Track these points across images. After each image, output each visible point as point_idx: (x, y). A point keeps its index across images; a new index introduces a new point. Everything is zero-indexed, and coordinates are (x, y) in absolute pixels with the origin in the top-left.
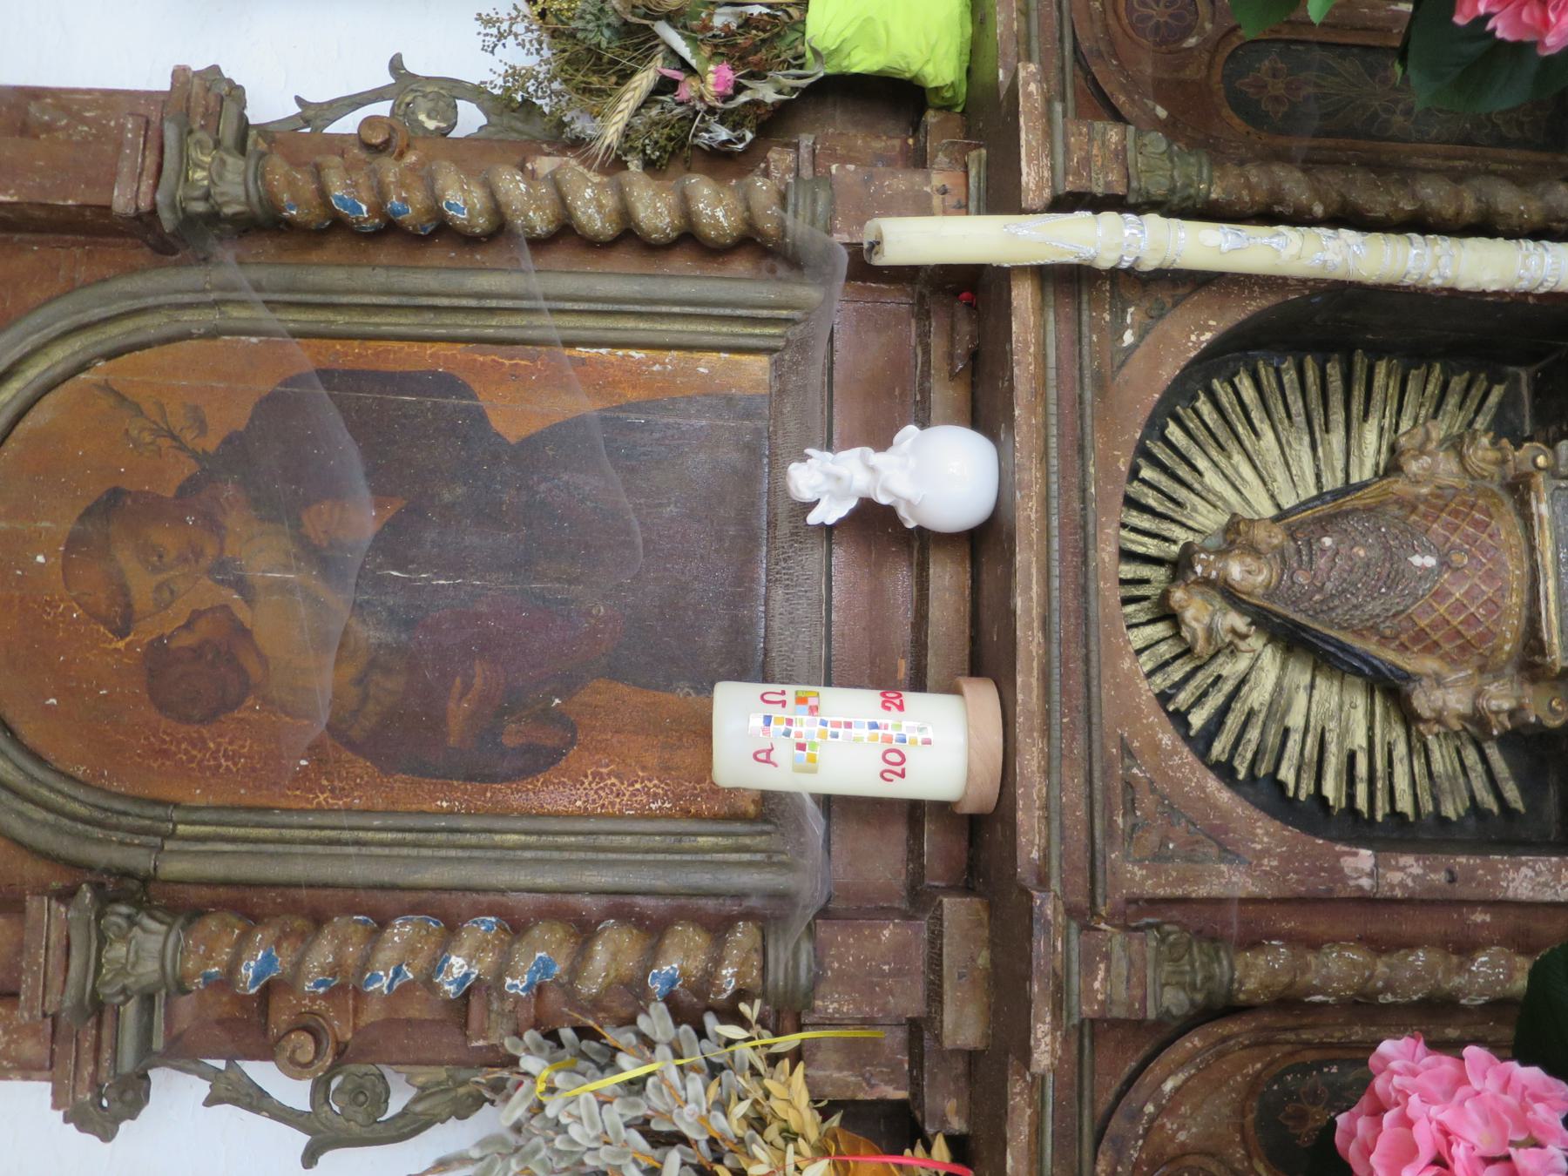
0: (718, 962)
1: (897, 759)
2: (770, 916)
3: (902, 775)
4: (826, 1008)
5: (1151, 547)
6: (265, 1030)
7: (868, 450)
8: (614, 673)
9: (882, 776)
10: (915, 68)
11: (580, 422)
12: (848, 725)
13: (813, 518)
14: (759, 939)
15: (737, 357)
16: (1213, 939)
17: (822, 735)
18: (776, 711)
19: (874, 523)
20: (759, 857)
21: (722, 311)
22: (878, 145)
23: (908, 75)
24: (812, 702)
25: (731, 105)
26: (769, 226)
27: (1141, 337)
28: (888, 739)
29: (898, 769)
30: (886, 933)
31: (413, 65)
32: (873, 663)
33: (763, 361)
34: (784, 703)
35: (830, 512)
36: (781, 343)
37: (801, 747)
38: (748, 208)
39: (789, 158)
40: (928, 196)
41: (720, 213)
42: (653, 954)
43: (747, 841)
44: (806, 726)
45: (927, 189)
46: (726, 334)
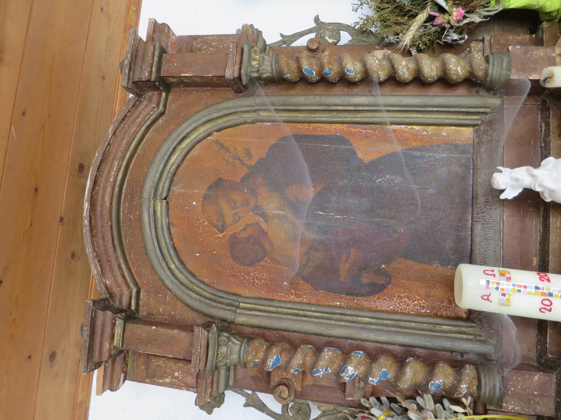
0: (459, 381)
1: (548, 303)
2: (483, 363)
3: (550, 310)
4: (508, 407)
6: (269, 383)
7: (531, 168)
8: (407, 256)
9: (540, 310)
10: (541, 4)
11: (394, 155)
12: (525, 287)
13: (502, 197)
14: (476, 373)
15: (459, 128)
17: (513, 290)
18: (491, 279)
19: (530, 199)
20: (470, 337)
21: (454, 109)
22: (519, 38)
23: (537, 7)
24: (507, 275)
25: (461, 24)
26: (480, 74)
28: (543, 294)
29: (548, 308)
30: (536, 377)
31: (322, 19)
32: (521, 258)
33: (470, 129)
34: (494, 275)
35: (510, 194)
36: (480, 122)
37: (504, 295)
38: (471, 66)
39: (480, 45)
40: (554, 58)
41: (459, 69)
42: (431, 374)
43: (464, 329)
44: (505, 285)
45: (554, 55)
46: (455, 119)
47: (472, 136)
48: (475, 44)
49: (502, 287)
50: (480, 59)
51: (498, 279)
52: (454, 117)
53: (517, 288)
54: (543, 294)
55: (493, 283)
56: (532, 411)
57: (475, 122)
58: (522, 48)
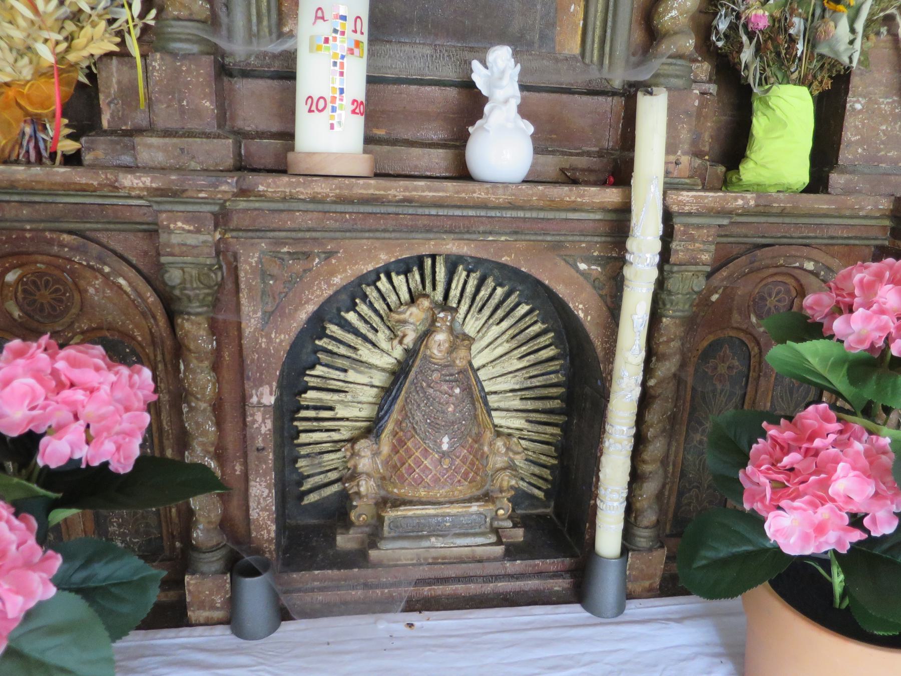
1: (321, 106)
3: (310, 111)
4: (155, 61)
5: (455, 293)
7: (519, 101)
9: (310, 97)
10: (753, 156)
12: (342, 74)
13: (476, 64)
14: (199, 18)
15: (580, 32)
16: (215, 304)
17: (335, 54)
18: (349, 25)
19: (472, 104)
20: (255, 28)
21: (610, 19)
22: (706, 137)
23: (748, 152)
24: (356, 51)
25: (741, 31)
26: (663, 46)
27: (583, 273)
28: (334, 99)
29: (314, 108)
30: (208, 104)
32: (383, 112)
33: (577, 50)
34: (355, 31)
35: (479, 76)
36: (587, 61)
37: (327, 40)
38: (676, 33)
39: (703, 76)
40: (675, 153)
41: (674, 13)
43: (265, 23)
44: (342, 45)
45: (679, 153)
46: (595, 24)
47: (566, 52)
48: (707, 69)
49: (338, 39)
50: (685, 46)
51: (350, 36)
52: (598, 23)
53: (339, 61)
54: (334, 99)
55: (343, 26)
56: (156, 98)
57: (588, 54)
58: (694, 109)
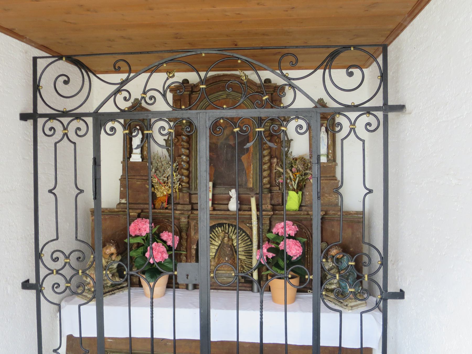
0: (185, 183)
2: (189, 188)
5: (230, 231)
6: (178, 135)
8: (215, 170)
11: (243, 165)
16: (187, 231)
27: (248, 226)
31: (292, 142)
42: (186, 176)
